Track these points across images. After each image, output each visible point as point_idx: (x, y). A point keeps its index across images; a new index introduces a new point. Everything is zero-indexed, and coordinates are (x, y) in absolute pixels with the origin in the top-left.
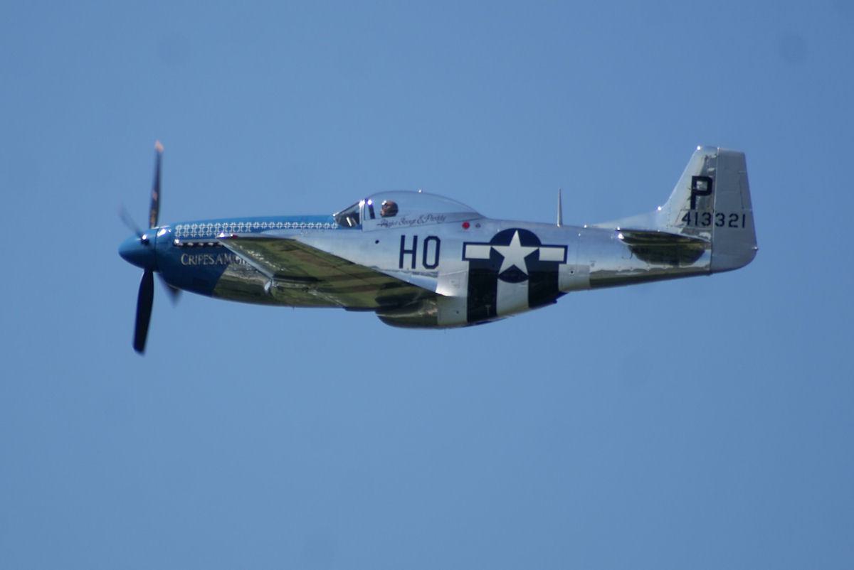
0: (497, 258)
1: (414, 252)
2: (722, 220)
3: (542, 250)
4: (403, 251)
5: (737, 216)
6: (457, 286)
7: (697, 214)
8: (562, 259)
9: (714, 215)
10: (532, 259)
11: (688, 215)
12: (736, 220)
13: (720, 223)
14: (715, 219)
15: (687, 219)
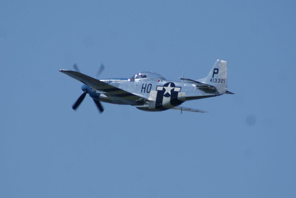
0: (164, 90)
1: (145, 88)
2: (219, 81)
3: (175, 88)
4: (143, 88)
5: (223, 80)
6: (154, 98)
7: (214, 79)
8: (179, 91)
9: (218, 79)
10: (172, 91)
11: (212, 79)
12: (223, 81)
13: (219, 82)
14: (218, 81)
15: (211, 81)
